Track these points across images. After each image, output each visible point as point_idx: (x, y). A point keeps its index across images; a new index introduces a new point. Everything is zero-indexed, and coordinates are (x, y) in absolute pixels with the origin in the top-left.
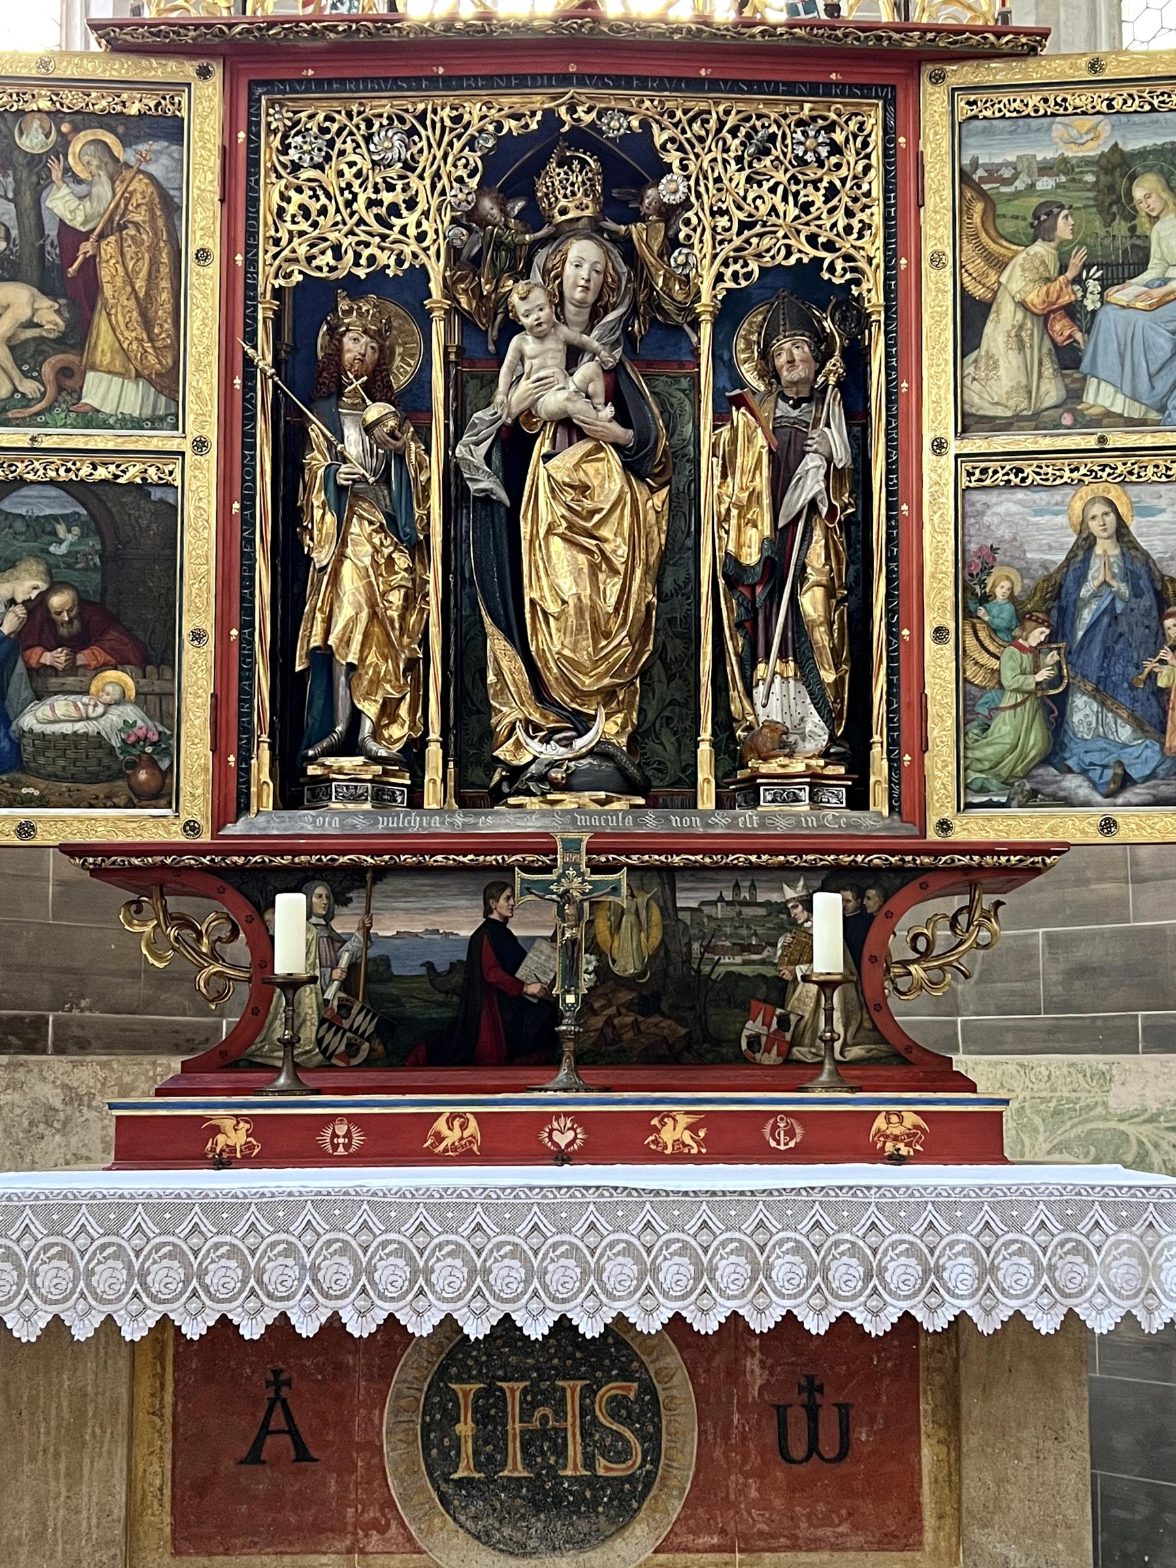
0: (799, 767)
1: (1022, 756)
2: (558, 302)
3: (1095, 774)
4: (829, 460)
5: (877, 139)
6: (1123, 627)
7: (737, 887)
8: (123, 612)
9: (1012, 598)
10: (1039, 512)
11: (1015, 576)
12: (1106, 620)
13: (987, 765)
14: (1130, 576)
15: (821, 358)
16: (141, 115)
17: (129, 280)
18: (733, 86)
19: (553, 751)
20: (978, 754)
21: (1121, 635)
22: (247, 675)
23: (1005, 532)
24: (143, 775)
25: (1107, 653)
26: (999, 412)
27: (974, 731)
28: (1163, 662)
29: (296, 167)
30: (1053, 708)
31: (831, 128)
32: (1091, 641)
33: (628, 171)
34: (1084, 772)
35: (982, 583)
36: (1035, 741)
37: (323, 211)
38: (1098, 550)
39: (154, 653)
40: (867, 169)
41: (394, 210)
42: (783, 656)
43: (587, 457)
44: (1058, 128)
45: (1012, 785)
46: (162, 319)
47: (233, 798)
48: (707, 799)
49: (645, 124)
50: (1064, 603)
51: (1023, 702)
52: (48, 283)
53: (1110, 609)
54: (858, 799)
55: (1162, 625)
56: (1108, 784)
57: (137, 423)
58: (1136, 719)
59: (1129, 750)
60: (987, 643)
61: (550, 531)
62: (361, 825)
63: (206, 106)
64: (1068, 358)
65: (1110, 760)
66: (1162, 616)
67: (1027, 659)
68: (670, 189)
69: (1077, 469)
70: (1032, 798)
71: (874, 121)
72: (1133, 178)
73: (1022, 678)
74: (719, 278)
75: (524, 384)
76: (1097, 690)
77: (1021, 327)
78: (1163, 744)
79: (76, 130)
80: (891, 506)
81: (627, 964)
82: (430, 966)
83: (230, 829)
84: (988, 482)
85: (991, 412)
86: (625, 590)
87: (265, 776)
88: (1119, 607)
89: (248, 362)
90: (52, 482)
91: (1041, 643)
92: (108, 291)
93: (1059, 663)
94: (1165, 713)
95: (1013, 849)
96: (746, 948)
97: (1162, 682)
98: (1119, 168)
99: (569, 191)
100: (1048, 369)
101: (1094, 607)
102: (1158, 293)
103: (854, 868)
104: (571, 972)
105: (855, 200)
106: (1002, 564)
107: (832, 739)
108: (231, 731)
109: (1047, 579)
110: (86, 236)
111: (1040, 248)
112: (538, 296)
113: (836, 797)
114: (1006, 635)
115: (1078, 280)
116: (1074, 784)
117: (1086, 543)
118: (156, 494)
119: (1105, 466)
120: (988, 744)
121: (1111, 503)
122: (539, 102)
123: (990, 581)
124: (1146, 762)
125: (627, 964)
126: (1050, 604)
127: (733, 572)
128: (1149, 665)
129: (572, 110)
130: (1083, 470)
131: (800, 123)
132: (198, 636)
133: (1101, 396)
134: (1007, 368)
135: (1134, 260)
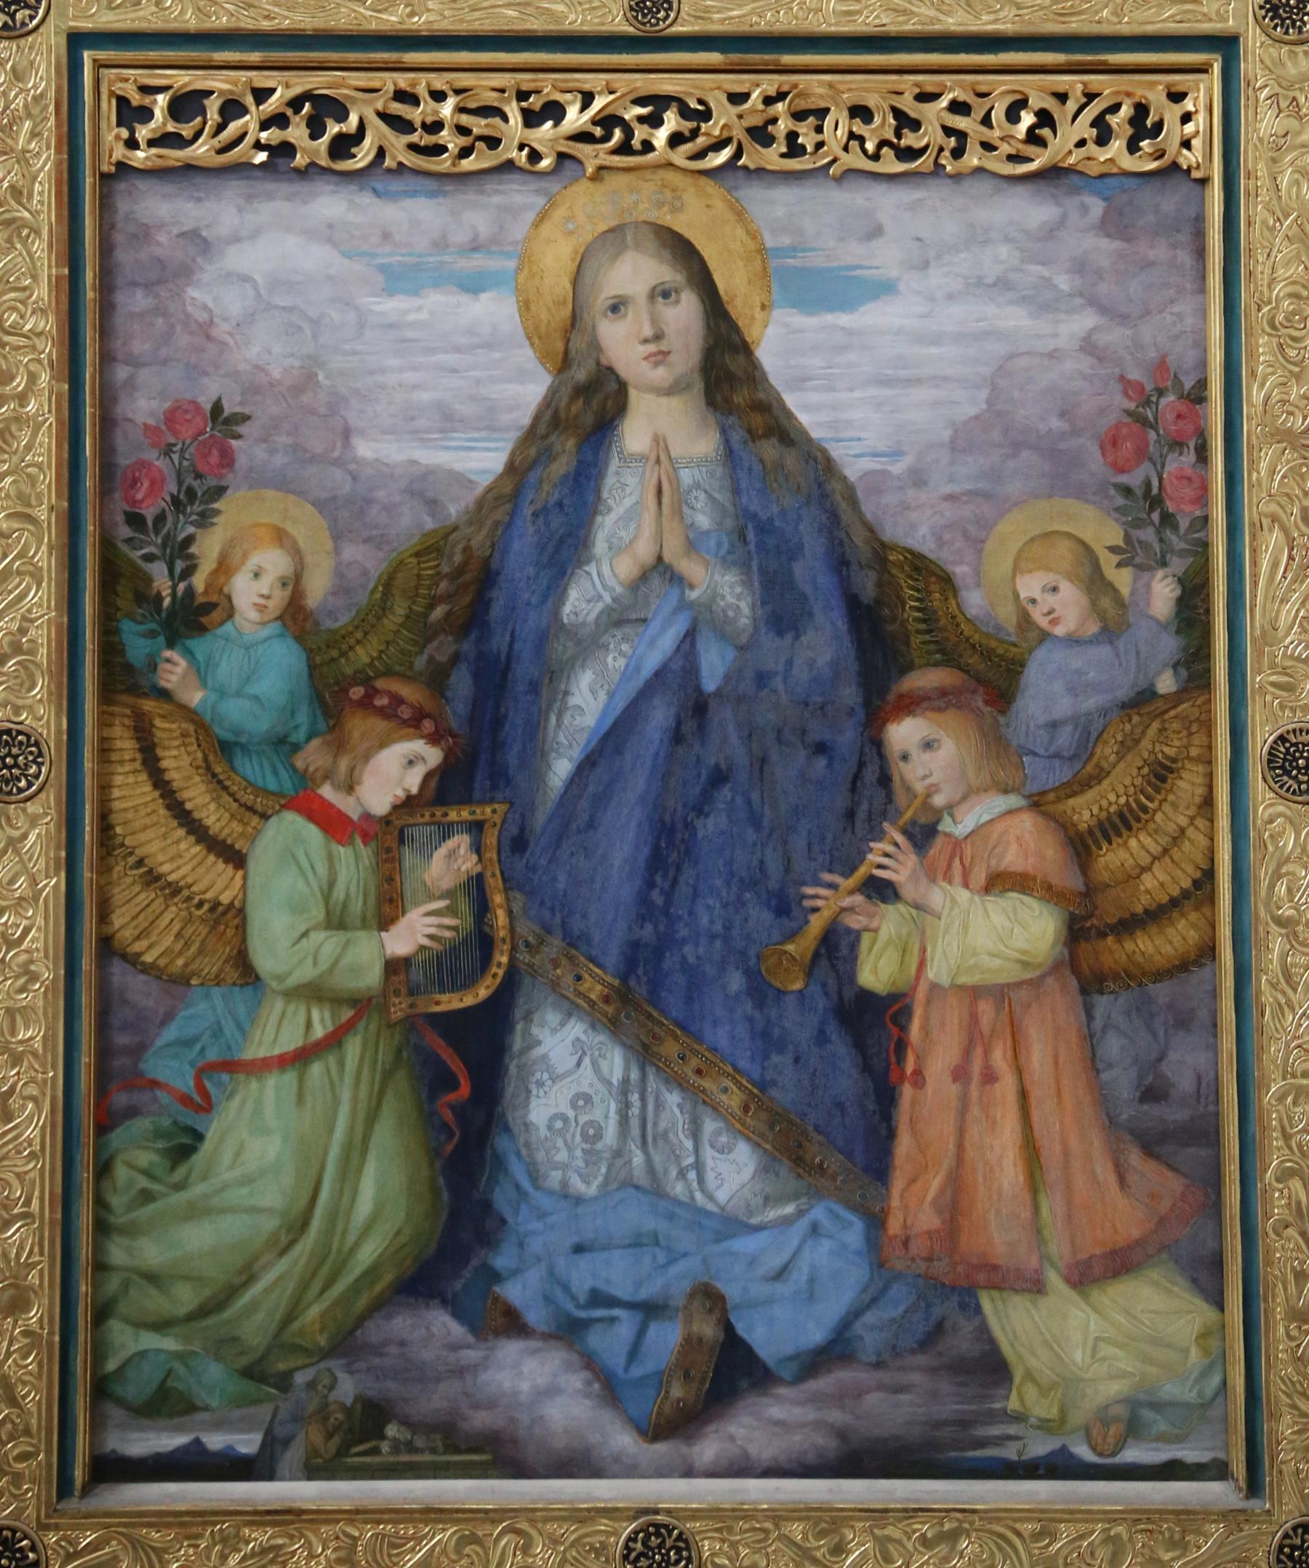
1: (328, 1264)
3: (612, 1341)
6: (726, 741)
9: (294, 615)
10: (399, 279)
11: (308, 527)
12: (660, 716)
13: (186, 1298)
14: (757, 543)
20: (151, 1253)
21: (719, 778)
23: (265, 350)
25: (668, 848)
27: (136, 1153)
28: (880, 890)
32: (602, 800)
34: (569, 1331)
35: (180, 554)
36: (381, 1198)
38: (635, 434)
45: (283, 1383)
50: (499, 642)
51: (334, 1041)
55: (878, 744)
56: (661, 1380)
58: (775, 1117)
59: (745, 1244)
60: (197, 796)
65: (675, 1281)
66: (879, 705)
67: (353, 867)
69: (555, 111)
70: (360, 1438)
73: (329, 944)
76: (622, 996)
78: (876, 1221)
84: (202, 150)
88: (714, 665)
91: (408, 804)
93: (476, 889)
94: (886, 1097)
97: (876, 971)
101: (615, 662)
106: (260, 480)
109: (432, 547)
116: (530, 1381)
119: (658, 104)
120: (194, 1212)
121: (682, 251)
123: (209, 547)
124: (811, 1294)
126: (442, 648)
128: (830, 899)
130: (575, 118)
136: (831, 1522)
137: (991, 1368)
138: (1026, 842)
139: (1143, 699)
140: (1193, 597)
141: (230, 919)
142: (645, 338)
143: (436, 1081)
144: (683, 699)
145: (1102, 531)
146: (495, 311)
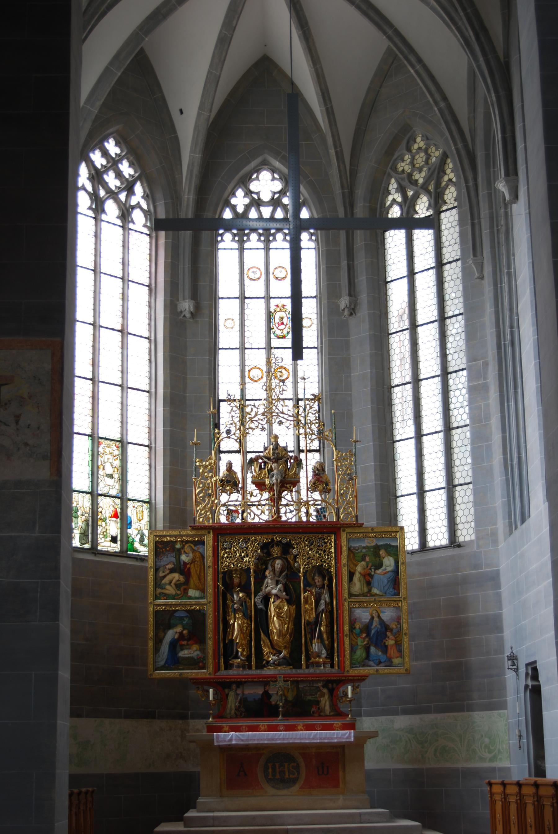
0: (321, 660)
2: (274, 573)
4: (326, 601)
5: (333, 540)
7: (310, 684)
8: (196, 634)
9: (359, 628)
14: (380, 624)
15: (324, 579)
16: (198, 540)
17: (196, 571)
18: (306, 533)
19: (275, 658)
22: (219, 645)
23: (358, 616)
24: (201, 664)
26: (356, 593)
29: (226, 549)
30: (367, 649)
31: (324, 539)
33: (286, 548)
34: (373, 661)
36: (364, 655)
37: (231, 557)
39: (201, 641)
40: (332, 546)
41: (244, 557)
42: (318, 638)
43: (281, 602)
44: (366, 541)
46: (202, 578)
47: (217, 668)
48: (304, 666)
49: (290, 540)
52: (181, 573)
53: (377, 630)
54: (332, 666)
57: (198, 598)
61: (274, 616)
62: (240, 673)
63: (209, 539)
64: (369, 583)
66: (386, 632)
67: (362, 640)
68: (294, 551)
70: (363, 666)
71: (333, 537)
72: (380, 550)
74: (304, 567)
75: (268, 588)
77: (360, 578)
79: (186, 544)
80: (337, 611)
81: (290, 698)
82: (254, 699)
83: (217, 674)
85: (355, 593)
86: (288, 628)
87: (223, 664)
89: (218, 586)
90: (183, 610)
92: (192, 574)
95: (359, 676)
96: (312, 695)
97: (386, 644)
98: (377, 548)
99: (276, 551)
100: (365, 586)
102: (385, 571)
103: (331, 680)
104: (281, 699)
105: (329, 552)
107: (328, 654)
108: (216, 656)
110: (188, 564)
111: (363, 563)
112: (272, 573)
113: (328, 666)
114: (359, 635)
115: (370, 569)
116: (371, 663)
117: (372, 618)
118: (202, 611)
122: (271, 536)
125: (290, 698)
127: (308, 623)
128: (384, 641)
129: (276, 538)
131: (319, 538)
132: (210, 638)
133: (375, 591)
134: (358, 586)
135: (379, 565)
136: (385, 669)
137: (392, 662)
138: (393, 638)
139: (398, 631)
140: (400, 627)
141: (357, 642)
142: (375, 615)
143: (366, 650)
144: (377, 632)
145: (396, 623)
146: (368, 614)
